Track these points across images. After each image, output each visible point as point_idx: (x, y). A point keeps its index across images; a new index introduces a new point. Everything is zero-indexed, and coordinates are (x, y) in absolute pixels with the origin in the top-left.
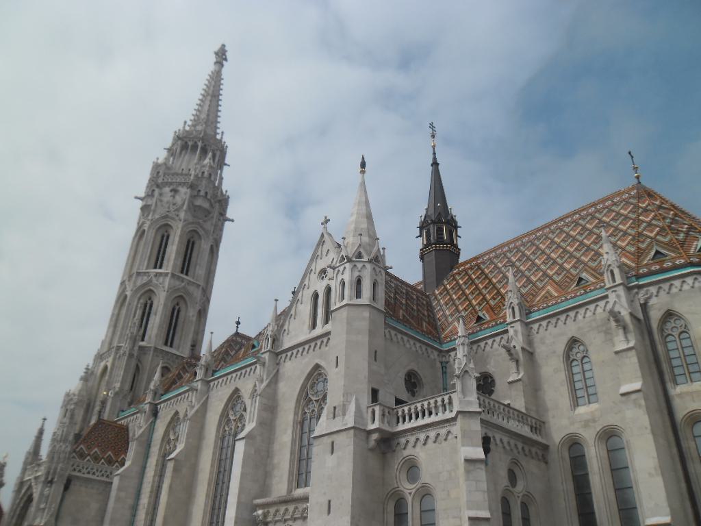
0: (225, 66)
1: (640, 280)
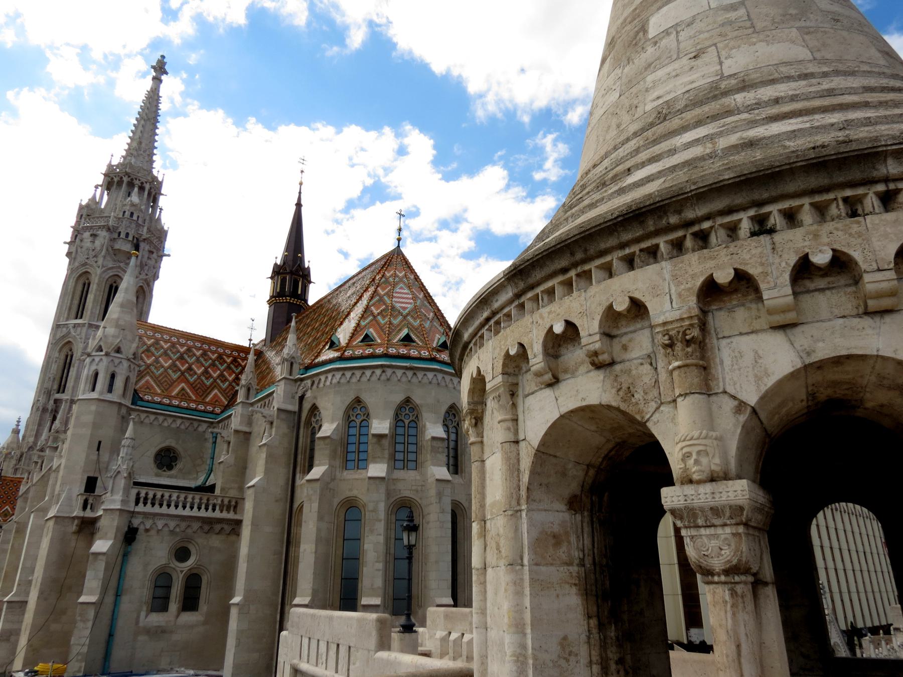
0: (163, 82)
1: (309, 371)
